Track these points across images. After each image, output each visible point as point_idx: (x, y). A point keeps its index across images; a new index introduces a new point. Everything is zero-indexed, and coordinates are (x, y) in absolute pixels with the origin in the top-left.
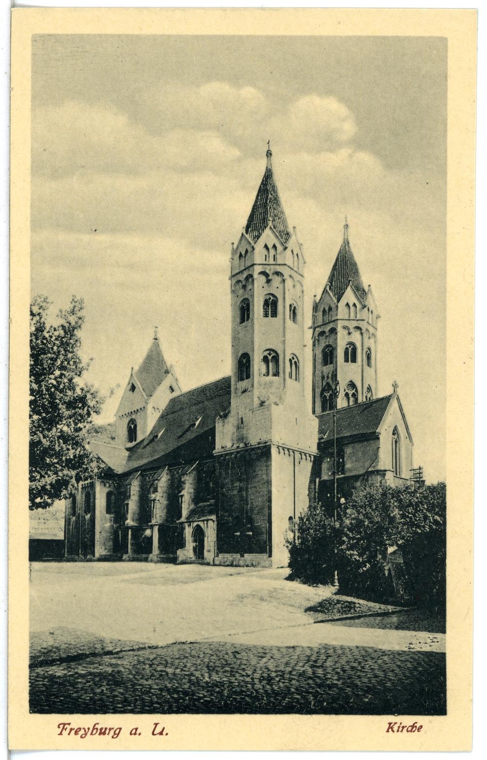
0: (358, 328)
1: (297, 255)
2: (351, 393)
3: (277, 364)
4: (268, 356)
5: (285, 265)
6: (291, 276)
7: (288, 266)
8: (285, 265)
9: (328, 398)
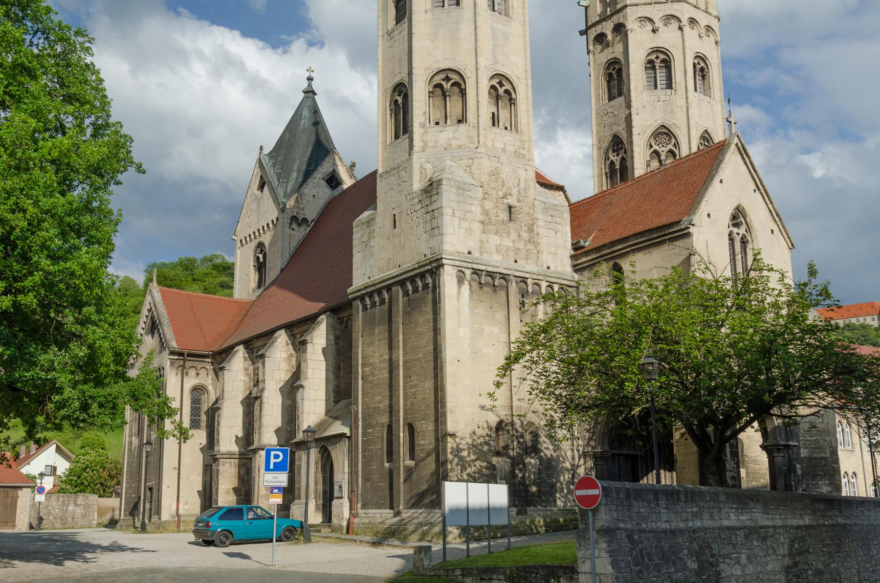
0: (670, 18)
2: (663, 150)
4: (444, 83)
9: (618, 167)
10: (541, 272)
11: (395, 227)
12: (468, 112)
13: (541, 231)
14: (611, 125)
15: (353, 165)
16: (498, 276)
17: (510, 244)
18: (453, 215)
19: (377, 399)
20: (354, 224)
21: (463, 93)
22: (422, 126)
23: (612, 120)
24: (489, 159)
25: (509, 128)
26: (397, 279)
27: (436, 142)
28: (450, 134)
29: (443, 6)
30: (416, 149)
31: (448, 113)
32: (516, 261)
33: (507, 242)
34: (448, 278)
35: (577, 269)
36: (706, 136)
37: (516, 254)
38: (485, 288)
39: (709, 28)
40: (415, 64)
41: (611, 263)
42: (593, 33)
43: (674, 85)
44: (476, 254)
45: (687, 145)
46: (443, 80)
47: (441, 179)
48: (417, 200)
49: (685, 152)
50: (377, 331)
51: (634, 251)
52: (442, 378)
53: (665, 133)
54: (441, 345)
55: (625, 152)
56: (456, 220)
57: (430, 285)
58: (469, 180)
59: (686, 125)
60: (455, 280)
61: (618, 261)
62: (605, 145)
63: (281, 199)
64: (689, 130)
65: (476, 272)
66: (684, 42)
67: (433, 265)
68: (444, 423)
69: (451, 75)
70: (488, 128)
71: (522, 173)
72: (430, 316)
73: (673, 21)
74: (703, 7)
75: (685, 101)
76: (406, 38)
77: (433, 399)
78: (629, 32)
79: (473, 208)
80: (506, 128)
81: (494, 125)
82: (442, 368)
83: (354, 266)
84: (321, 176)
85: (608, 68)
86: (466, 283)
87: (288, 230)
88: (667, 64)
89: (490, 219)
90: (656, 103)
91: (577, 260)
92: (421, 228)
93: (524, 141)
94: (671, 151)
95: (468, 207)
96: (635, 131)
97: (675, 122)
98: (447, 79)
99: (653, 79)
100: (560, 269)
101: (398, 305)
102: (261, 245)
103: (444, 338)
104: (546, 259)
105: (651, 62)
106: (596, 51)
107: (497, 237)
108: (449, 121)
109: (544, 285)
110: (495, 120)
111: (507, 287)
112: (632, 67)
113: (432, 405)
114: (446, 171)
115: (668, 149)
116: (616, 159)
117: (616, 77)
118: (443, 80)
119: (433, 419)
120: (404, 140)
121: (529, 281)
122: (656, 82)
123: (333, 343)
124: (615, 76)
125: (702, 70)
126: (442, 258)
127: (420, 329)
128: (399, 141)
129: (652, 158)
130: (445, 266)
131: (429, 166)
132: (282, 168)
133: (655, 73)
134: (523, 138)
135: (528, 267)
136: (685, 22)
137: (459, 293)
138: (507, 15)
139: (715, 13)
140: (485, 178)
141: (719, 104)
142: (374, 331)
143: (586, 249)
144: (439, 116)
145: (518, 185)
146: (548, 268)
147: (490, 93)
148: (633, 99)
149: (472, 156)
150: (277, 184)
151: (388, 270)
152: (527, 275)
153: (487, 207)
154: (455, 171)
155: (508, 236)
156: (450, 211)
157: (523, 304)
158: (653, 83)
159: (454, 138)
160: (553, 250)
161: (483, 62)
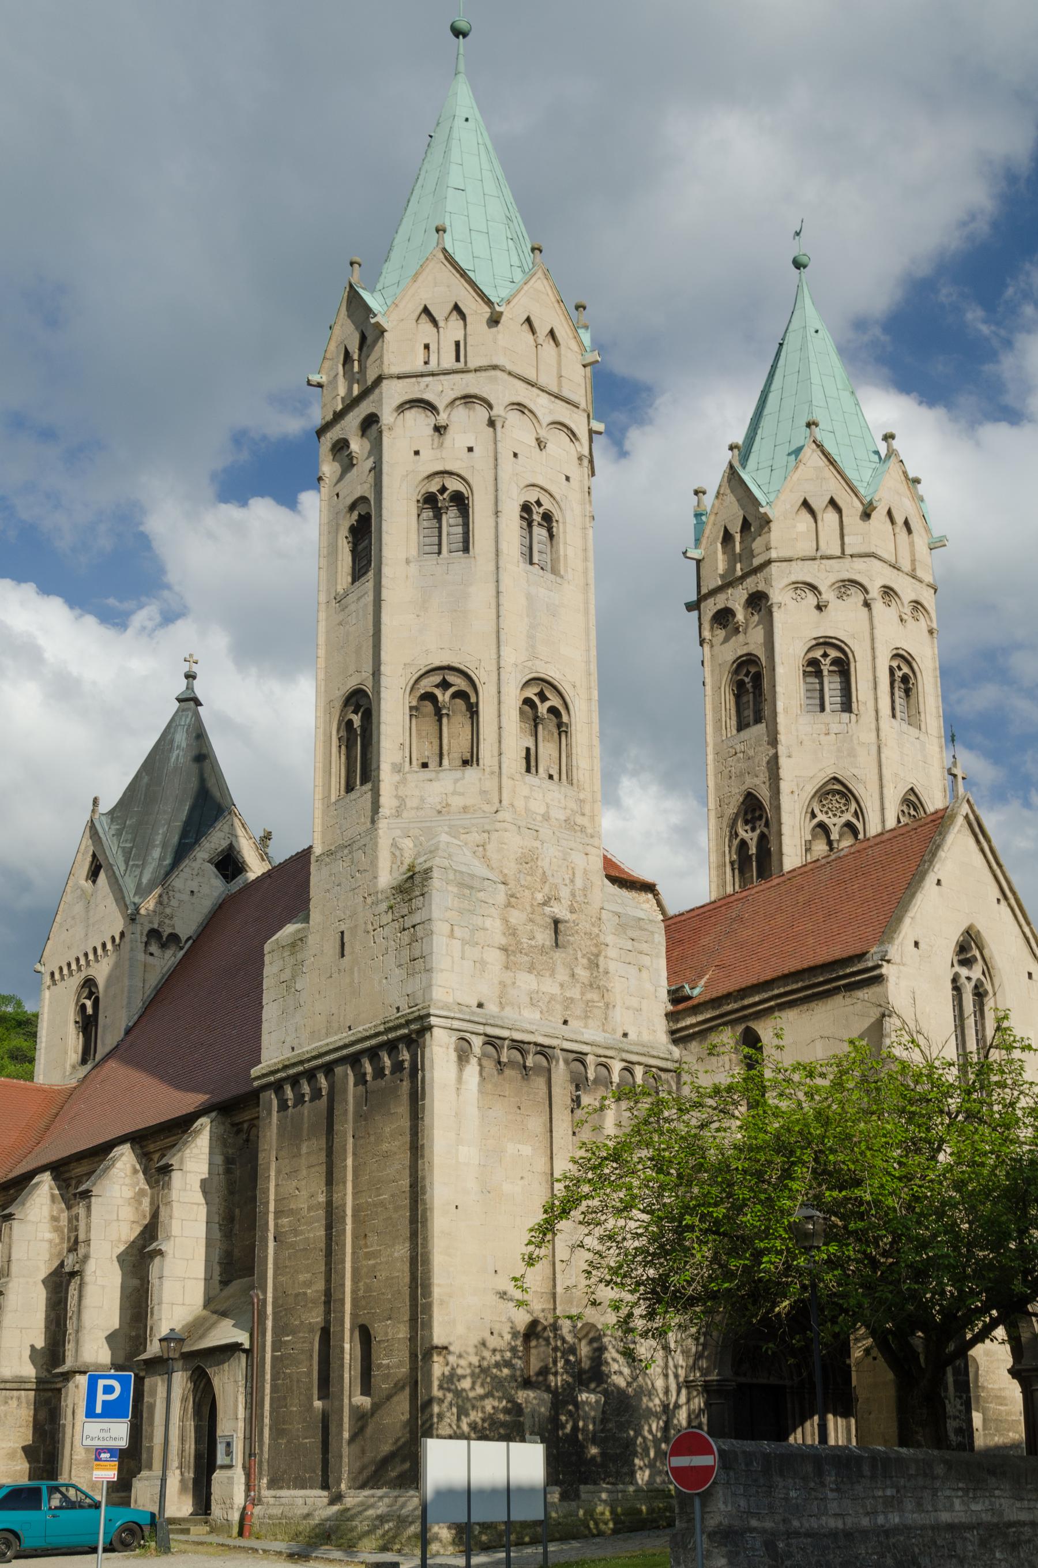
1: (552, 333)
2: (835, 823)
3: (472, 718)
4: (438, 692)
5: (495, 367)
6: (520, 407)
7: (510, 373)
8: (495, 367)
9: (753, 850)
10: (611, 1042)
11: (343, 955)
12: (481, 746)
13: (612, 966)
14: (741, 775)
15: (267, 837)
16: (533, 1049)
17: (556, 990)
18: (452, 935)
19: (302, 1278)
20: (267, 947)
21: (473, 711)
22: (397, 769)
23: (742, 765)
24: (519, 833)
25: (556, 777)
26: (345, 1052)
27: (422, 799)
28: (448, 786)
29: (439, 553)
30: (384, 811)
31: (445, 747)
32: (565, 1022)
33: (549, 986)
34: (440, 1052)
35: (678, 1038)
36: (913, 798)
37: (567, 1008)
38: (508, 1072)
39: (917, 605)
40: (384, 656)
41: (740, 1028)
42: (710, 607)
43: (854, 706)
44: (492, 1008)
45: (878, 813)
46: (437, 686)
47: (430, 869)
48: (384, 906)
49: (873, 828)
50: (304, 1150)
51: (781, 1007)
52: (425, 1239)
53: (839, 792)
54: (423, 1178)
55: (767, 825)
56: (457, 943)
57: (406, 1065)
58: (482, 871)
59: (876, 777)
60: (453, 1056)
61: (753, 1025)
62: (731, 810)
63: (131, 897)
64: (881, 787)
65: (491, 1041)
66: (872, 628)
67: (413, 1027)
68: (428, 1325)
69: (451, 678)
70: (518, 776)
71: (579, 860)
72: (405, 1123)
73: (853, 590)
74: (906, 566)
75: (874, 734)
76: (370, 609)
77: (407, 1280)
78: (775, 609)
79: (488, 923)
80: (551, 777)
81: (528, 770)
82: (425, 1221)
83: (265, 1027)
84: (206, 856)
85: (736, 672)
86: (474, 1061)
87: (141, 956)
88: (843, 667)
89: (519, 943)
90: (822, 737)
91: (677, 1021)
92: (391, 959)
93: (582, 801)
94: (848, 825)
95: (479, 921)
96: (785, 786)
97: (855, 771)
98: (445, 685)
99: (817, 694)
100: (646, 1037)
101: (346, 1102)
102: (89, 984)
103: (431, 1163)
104: (622, 1019)
105: (814, 663)
106: (714, 640)
107: (532, 977)
108: (445, 762)
109: (617, 1066)
110: (530, 761)
111: (549, 1071)
112: (780, 670)
113: (406, 1291)
114: (440, 853)
115: (843, 820)
116: (751, 838)
117: (750, 689)
118: (437, 686)
119: (407, 1318)
120: (362, 794)
121: (590, 1060)
122: (822, 698)
123: (221, 1169)
124: (749, 686)
125: (905, 679)
126: (429, 1015)
127: (385, 1147)
128: (353, 795)
129: (814, 836)
130: (435, 1030)
131: (407, 844)
132: (133, 840)
133: (822, 683)
134: (582, 796)
135: (588, 1034)
136: (875, 592)
137: (460, 1080)
138: (555, 571)
139: (928, 578)
140: (511, 868)
141: (935, 741)
142: (299, 1149)
143: (694, 1002)
144: (428, 751)
145: (572, 881)
146: (625, 1035)
147: (522, 712)
148: (781, 728)
149: (487, 827)
150: (122, 868)
151: (327, 1035)
152: (585, 1049)
153: (513, 921)
154: (455, 855)
155: (553, 974)
156: (445, 928)
157: (577, 1101)
158: (817, 702)
159: (455, 793)
160: (634, 1002)
161: (510, 656)
